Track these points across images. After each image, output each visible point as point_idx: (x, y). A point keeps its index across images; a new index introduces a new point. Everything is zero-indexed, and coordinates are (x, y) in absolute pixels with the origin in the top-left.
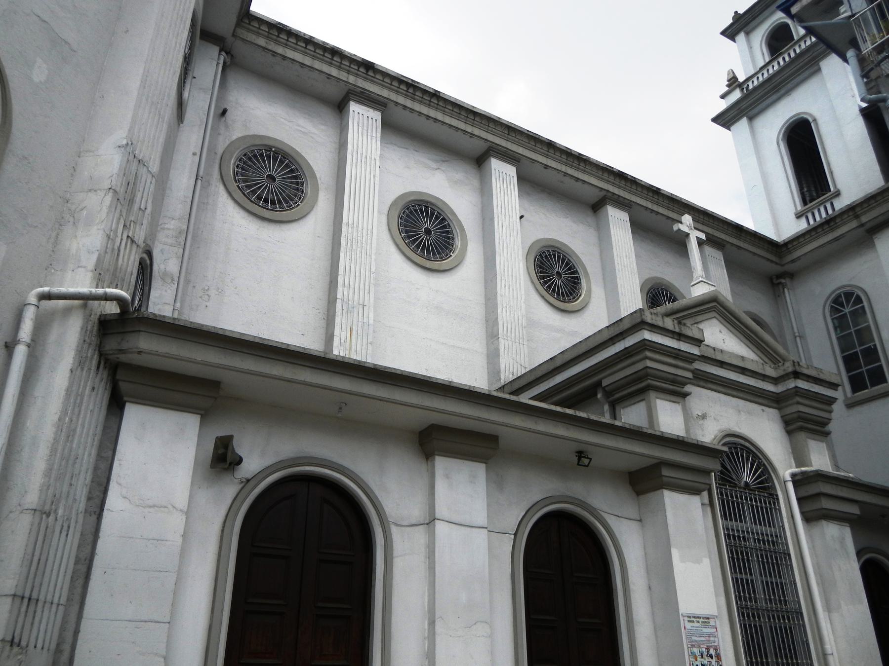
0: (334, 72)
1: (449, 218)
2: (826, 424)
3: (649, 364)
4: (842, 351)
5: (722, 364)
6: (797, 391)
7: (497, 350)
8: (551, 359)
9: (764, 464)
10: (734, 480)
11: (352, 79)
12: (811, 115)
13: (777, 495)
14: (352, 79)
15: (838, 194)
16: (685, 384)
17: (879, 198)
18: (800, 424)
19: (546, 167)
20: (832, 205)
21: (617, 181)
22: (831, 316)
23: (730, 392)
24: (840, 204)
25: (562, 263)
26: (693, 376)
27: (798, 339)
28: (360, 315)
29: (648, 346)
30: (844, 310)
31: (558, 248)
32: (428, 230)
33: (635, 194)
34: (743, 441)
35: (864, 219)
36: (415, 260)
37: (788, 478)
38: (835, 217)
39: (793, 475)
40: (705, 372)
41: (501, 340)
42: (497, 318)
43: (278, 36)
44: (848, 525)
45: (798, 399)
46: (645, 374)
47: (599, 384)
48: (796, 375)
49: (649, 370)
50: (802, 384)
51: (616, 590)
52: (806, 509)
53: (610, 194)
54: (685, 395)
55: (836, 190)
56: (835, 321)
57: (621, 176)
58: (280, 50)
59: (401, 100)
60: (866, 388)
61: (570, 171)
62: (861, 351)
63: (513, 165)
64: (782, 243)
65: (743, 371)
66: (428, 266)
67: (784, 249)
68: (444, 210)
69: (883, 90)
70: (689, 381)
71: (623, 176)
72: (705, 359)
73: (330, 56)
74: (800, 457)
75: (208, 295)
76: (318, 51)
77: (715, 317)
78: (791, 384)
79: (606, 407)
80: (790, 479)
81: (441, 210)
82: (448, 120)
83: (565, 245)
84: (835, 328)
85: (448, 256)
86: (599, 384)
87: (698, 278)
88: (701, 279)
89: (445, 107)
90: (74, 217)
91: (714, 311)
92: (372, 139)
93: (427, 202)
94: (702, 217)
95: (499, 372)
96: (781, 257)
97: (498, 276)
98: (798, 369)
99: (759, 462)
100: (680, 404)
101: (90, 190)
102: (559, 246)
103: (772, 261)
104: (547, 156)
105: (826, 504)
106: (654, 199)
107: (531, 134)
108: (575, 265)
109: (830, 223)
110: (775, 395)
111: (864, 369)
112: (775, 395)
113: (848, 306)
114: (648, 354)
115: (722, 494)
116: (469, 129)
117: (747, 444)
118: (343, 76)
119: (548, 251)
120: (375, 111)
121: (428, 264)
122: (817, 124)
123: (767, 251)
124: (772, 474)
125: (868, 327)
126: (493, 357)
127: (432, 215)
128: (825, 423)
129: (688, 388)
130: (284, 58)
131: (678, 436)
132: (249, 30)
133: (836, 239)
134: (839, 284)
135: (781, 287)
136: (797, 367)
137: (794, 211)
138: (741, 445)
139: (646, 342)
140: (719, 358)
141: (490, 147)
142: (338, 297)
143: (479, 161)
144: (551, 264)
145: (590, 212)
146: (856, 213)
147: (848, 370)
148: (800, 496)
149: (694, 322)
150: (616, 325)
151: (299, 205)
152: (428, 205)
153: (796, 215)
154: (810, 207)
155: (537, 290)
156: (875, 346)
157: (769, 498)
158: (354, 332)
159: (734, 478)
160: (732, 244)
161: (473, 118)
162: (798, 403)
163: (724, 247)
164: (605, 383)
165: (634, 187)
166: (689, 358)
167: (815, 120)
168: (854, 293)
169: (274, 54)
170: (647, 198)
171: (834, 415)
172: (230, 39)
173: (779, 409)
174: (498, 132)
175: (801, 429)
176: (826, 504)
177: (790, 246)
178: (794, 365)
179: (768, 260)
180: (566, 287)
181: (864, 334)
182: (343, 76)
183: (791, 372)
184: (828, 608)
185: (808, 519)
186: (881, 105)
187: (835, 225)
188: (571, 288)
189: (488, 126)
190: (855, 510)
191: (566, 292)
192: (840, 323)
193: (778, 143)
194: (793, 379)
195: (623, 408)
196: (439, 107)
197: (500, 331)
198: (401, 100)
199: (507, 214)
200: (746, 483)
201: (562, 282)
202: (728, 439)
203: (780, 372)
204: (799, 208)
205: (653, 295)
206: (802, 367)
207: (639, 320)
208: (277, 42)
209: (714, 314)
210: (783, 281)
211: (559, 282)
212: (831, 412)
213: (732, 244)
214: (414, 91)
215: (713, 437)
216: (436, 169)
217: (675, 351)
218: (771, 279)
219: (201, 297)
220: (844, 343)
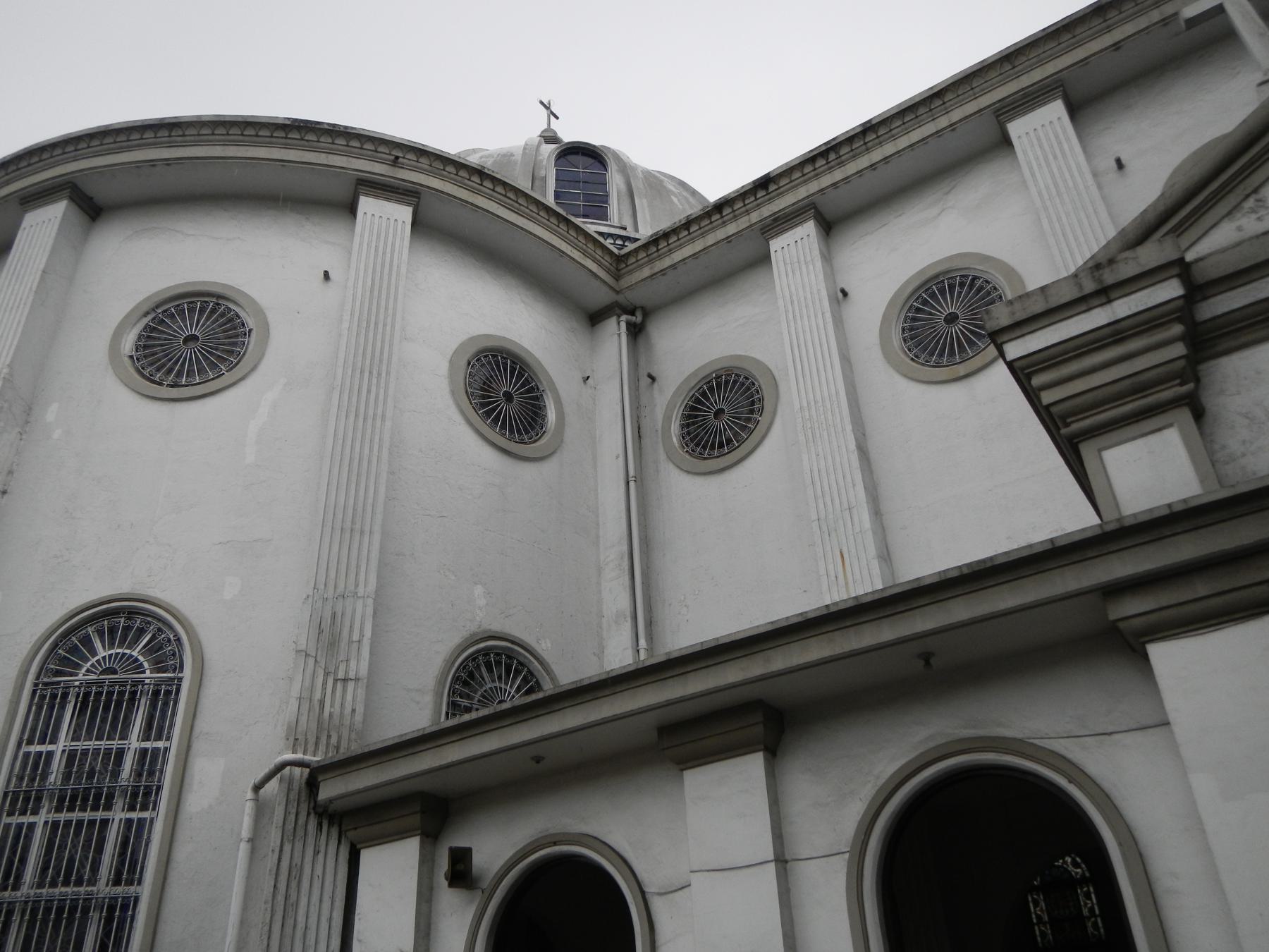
0: (732, 229)
11: (755, 217)
14: (755, 217)
19: (1116, 46)
29: (1028, 367)
32: (949, 317)
43: (658, 250)
58: (667, 262)
59: (826, 181)
73: (718, 216)
75: (685, 606)
76: (703, 224)
82: (903, 142)
89: (891, 130)
93: (937, 276)
104: (1109, 29)
118: (743, 223)
120: (805, 225)
121: (962, 369)
130: (674, 267)
131: (1169, 506)
132: (630, 272)
149: (1241, 197)
158: (846, 556)
169: (663, 272)
172: (620, 298)
174: (994, 81)
182: (743, 223)
196: (881, 139)
198: (826, 181)
208: (660, 258)
214: (837, 153)
216: (939, 214)
219: (679, 613)
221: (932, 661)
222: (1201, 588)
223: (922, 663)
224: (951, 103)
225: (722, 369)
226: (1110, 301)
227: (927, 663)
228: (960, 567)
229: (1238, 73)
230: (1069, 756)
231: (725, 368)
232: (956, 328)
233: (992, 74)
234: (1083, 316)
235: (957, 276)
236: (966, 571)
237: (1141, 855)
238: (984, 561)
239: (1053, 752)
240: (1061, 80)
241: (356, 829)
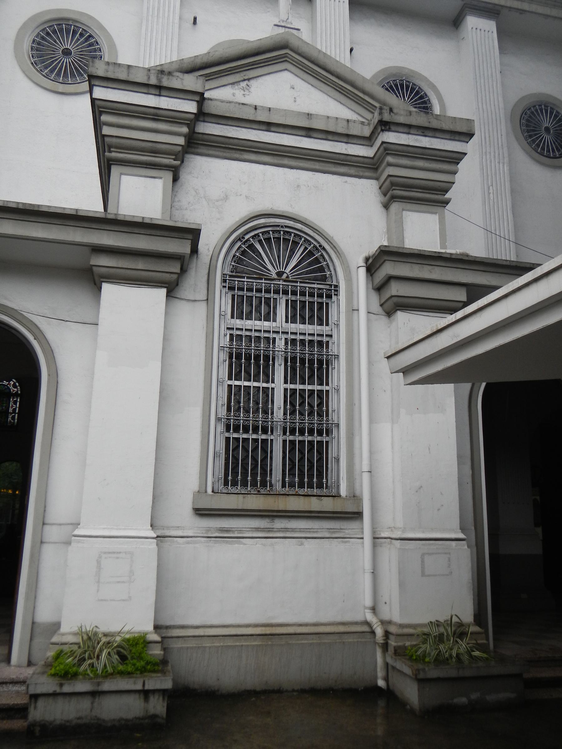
5: (268, 126)
23: (286, 161)
32: (66, 50)
34: (292, 222)
45: (390, 159)
66: (60, 91)
77: (286, 70)
91: (286, 61)
93: (68, 20)
98: (387, 117)
100: (437, 214)
110: (366, 160)
117: (299, 226)
121: (61, 88)
131: (143, 218)
149: (242, 79)
160: (510, 8)
163: (498, 14)
173: (377, 179)
206: (396, 114)
212: (455, 173)
226: (160, 95)
228: (18, 203)
229: (269, 12)
230: (40, 326)
232: (66, 60)
234: (143, 95)
235: (81, 28)
236: (21, 207)
237: (57, 382)
238: (33, 205)
239: (32, 321)
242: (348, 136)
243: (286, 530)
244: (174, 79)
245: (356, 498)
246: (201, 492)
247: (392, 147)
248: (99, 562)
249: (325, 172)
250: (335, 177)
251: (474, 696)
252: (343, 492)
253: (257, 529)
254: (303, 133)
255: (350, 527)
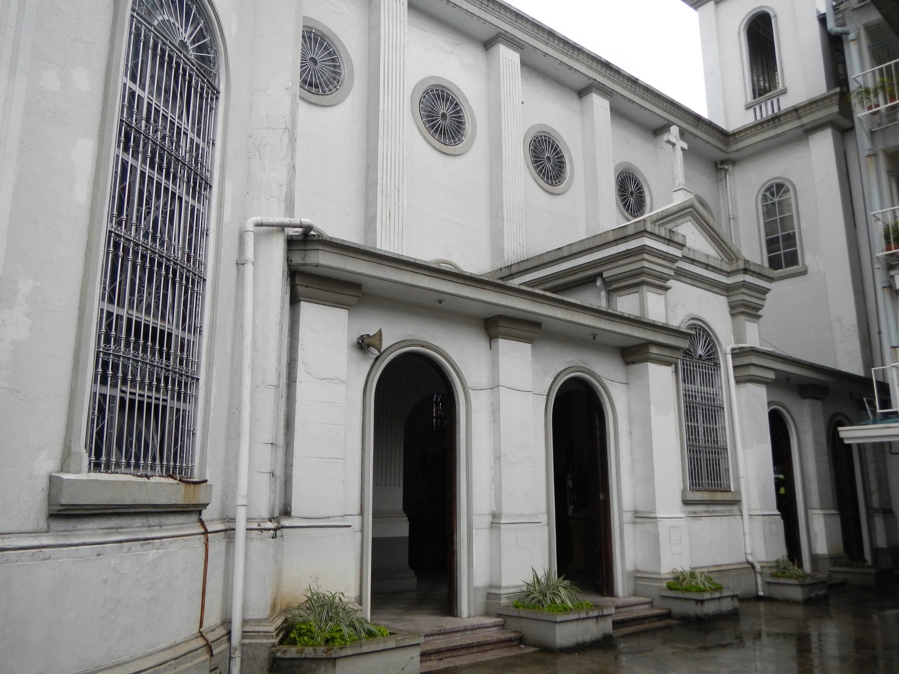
1: (462, 104)
2: (758, 309)
3: (646, 264)
4: (767, 235)
6: (744, 284)
7: (501, 231)
8: (559, 249)
9: (714, 341)
10: (691, 352)
12: (772, 10)
13: (720, 364)
15: (784, 92)
16: (668, 280)
17: (820, 103)
18: (742, 309)
19: (546, 54)
20: (778, 100)
21: (603, 70)
22: (762, 203)
23: (696, 283)
24: (787, 103)
25: (552, 148)
26: (675, 273)
27: (732, 220)
28: (397, 199)
30: (773, 198)
31: (549, 134)
33: (617, 83)
35: (805, 120)
36: (437, 147)
37: (728, 350)
38: (780, 116)
39: (733, 349)
40: (681, 268)
41: (505, 222)
42: (502, 202)
44: (765, 386)
45: (744, 290)
46: (640, 272)
47: (600, 274)
48: (746, 271)
49: (645, 269)
50: (749, 279)
51: (609, 434)
52: (738, 375)
53: (597, 83)
54: (667, 289)
55: (784, 88)
56: (764, 208)
57: (607, 66)
60: (781, 268)
61: (566, 60)
62: (782, 236)
63: (518, 52)
64: (731, 133)
65: (707, 266)
66: (445, 151)
67: (732, 138)
68: (457, 95)
69: (847, 22)
70: (671, 277)
71: (609, 66)
72: (685, 258)
74: (739, 335)
77: (690, 220)
78: (740, 278)
79: (603, 293)
80: (730, 352)
81: (456, 96)
83: (555, 131)
84: (764, 214)
85: (461, 141)
86: (600, 274)
87: (679, 184)
88: (682, 187)
90: (259, 151)
92: (400, 23)
93: (444, 87)
94: (669, 106)
95: (503, 251)
96: (727, 145)
97: (504, 163)
98: (747, 267)
99: (710, 339)
101: (269, 128)
102: (549, 131)
103: (720, 150)
104: (547, 44)
105: (754, 371)
106: (632, 88)
107: (536, 22)
108: (562, 150)
109: (775, 119)
111: (782, 252)
112: (725, 285)
113: (777, 195)
114: (646, 256)
115: (683, 364)
116: (483, 15)
117: (704, 326)
119: (541, 136)
122: (776, 20)
123: (718, 139)
124: (718, 348)
125: (791, 216)
126: (497, 236)
127: (447, 99)
128: (758, 308)
129: (671, 283)
133: (778, 135)
134: (772, 176)
135: (723, 172)
136: (747, 264)
137: (744, 102)
138: (700, 326)
139: (646, 247)
140: (691, 257)
141: (499, 33)
142: (378, 182)
143: (487, 45)
144: (543, 149)
145: (576, 97)
146: (798, 114)
147: (769, 251)
148: (736, 365)
150: (621, 229)
151: (338, 89)
152: (444, 90)
153: (745, 106)
154: (759, 101)
155: (531, 174)
156: (794, 233)
157: (714, 366)
158: (392, 215)
159: (692, 350)
160: (691, 133)
161: (487, 4)
162: (744, 293)
164: (605, 275)
165: (617, 76)
166: (672, 259)
167: (775, 16)
168: (784, 185)
170: (626, 87)
171: (766, 303)
173: (727, 296)
175: (743, 313)
176: (754, 371)
177: (737, 136)
178: (745, 264)
179: (717, 147)
180: (554, 171)
181: (786, 222)
183: (741, 269)
184: (744, 447)
185: (738, 381)
186: (844, 37)
187: (779, 123)
188: (557, 171)
189: (499, 12)
190: (771, 375)
191: (551, 176)
192: (769, 211)
193: (739, 33)
194: (742, 275)
195: (619, 296)
197: (505, 214)
199: (512, 102)
200: (700, 356)
201: (551, 166)
202: (691, 322)
203: (734, 268)
204: (750, 99)
205: (622, 179)
207: (643, 229)
209: (690, 218)
210: (726, 167)
211: (549, 166)
212: (764, 300)
213: (691, 133)
215: (681, 320)
216: (451, 53)
217: (665, 254)
218: (716, 164)
220: (770, 227)
221: (596, 337)
222: (666, 353)
223: (592, 337)
224: (490, 9)
225: (321, 32)
226: (669, 245)
227: (594, 338)
231: (323, 33)
233: (508, 15)
234: (661, 244)
240: (524, 46)
241: (307, 287)
242: (721, 270)
243: (714, 512)
244: (675, 235)
245: (738, 492)
246: (684, 491)
247: (746, 283)
248: (669, 532)
249: (709, 291)
250: (712, 294)
251: (816, 592)
252: (732, 489)
253: (705, 512)
254: (704, 267)
255: (735, 508)
